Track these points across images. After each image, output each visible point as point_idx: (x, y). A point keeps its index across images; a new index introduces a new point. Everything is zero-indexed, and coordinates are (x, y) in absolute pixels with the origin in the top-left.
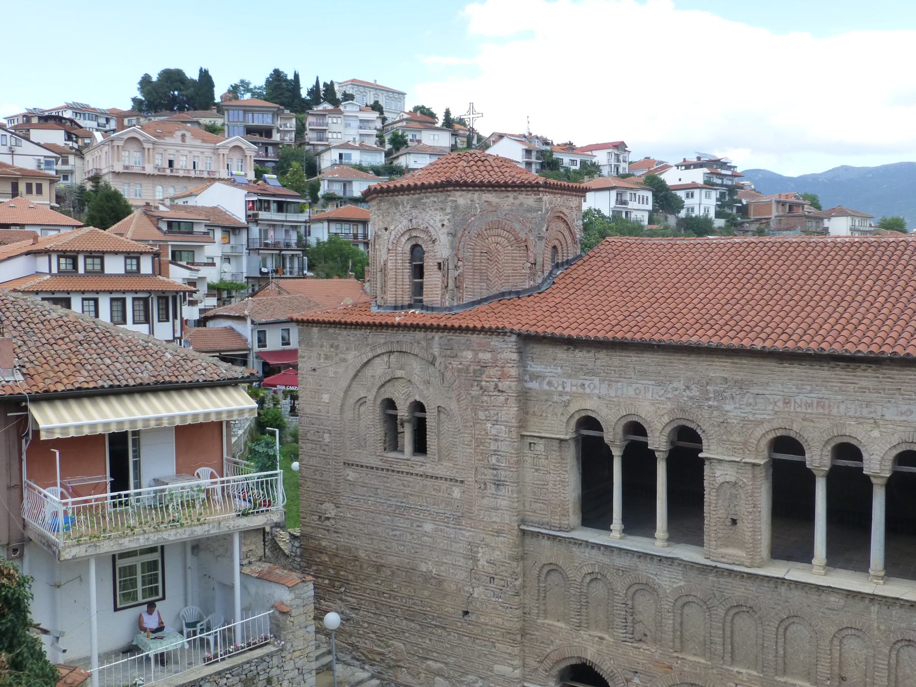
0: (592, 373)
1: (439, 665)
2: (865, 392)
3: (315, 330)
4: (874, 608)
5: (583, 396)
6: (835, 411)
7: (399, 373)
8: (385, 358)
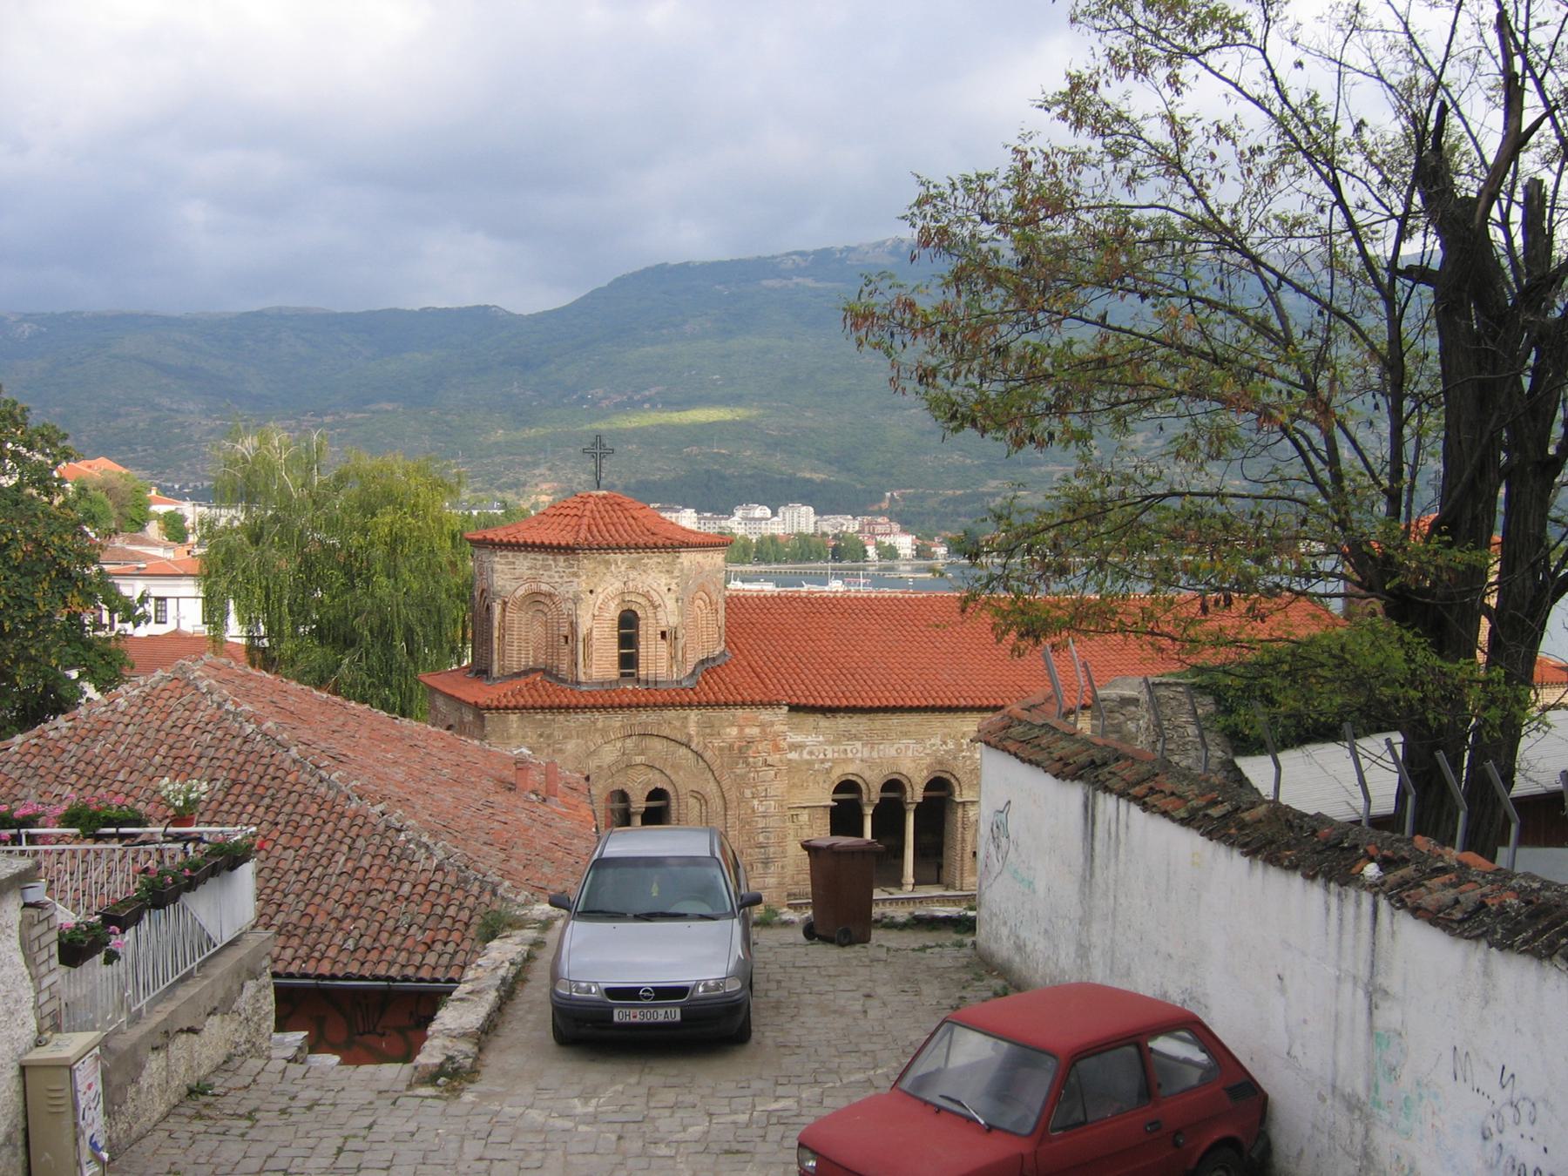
0: (856, 738)
3: (514, 718)
5: (845, 761)
7: (639, 759)
8: (619, 744)
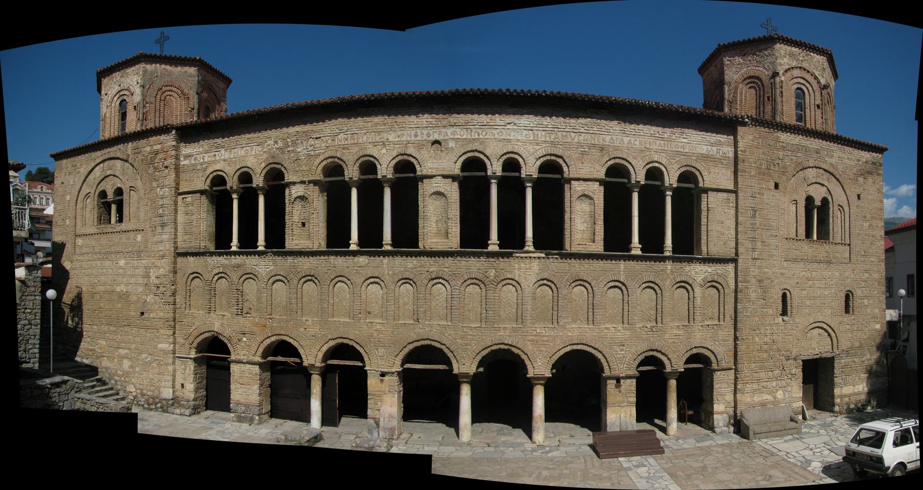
1: (126, 351)
2: (377, 126)
6: (360, 141)
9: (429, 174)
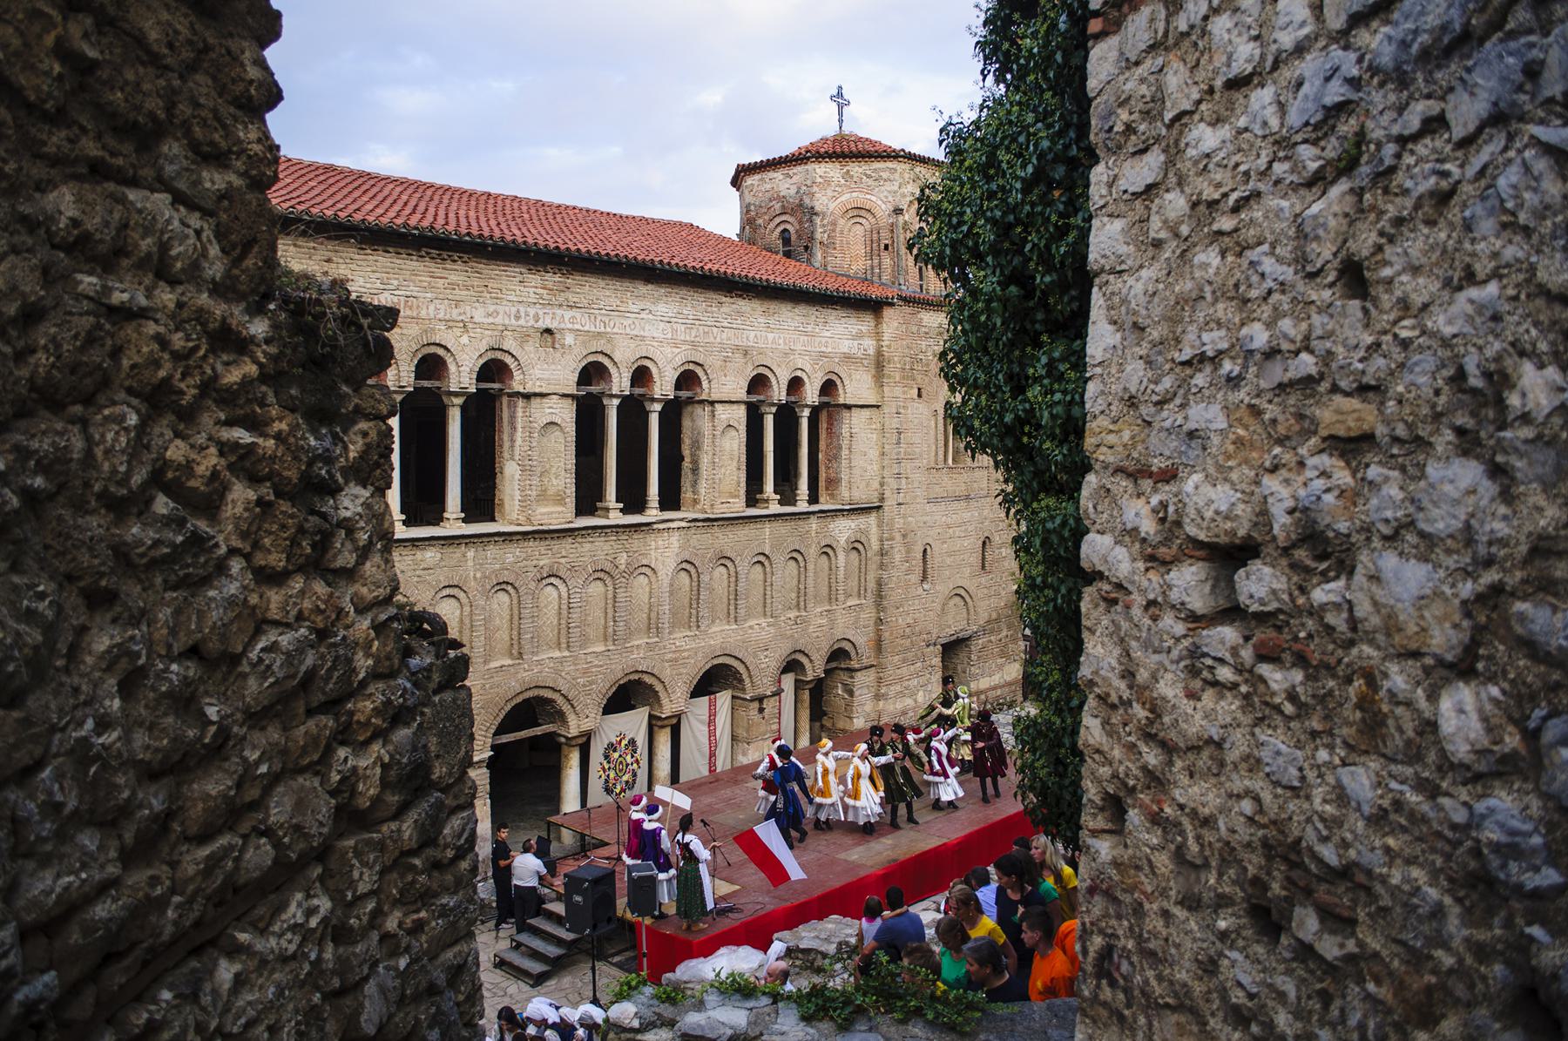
4: (471, 554)
6: (423, 313)
9: (537, 390)
